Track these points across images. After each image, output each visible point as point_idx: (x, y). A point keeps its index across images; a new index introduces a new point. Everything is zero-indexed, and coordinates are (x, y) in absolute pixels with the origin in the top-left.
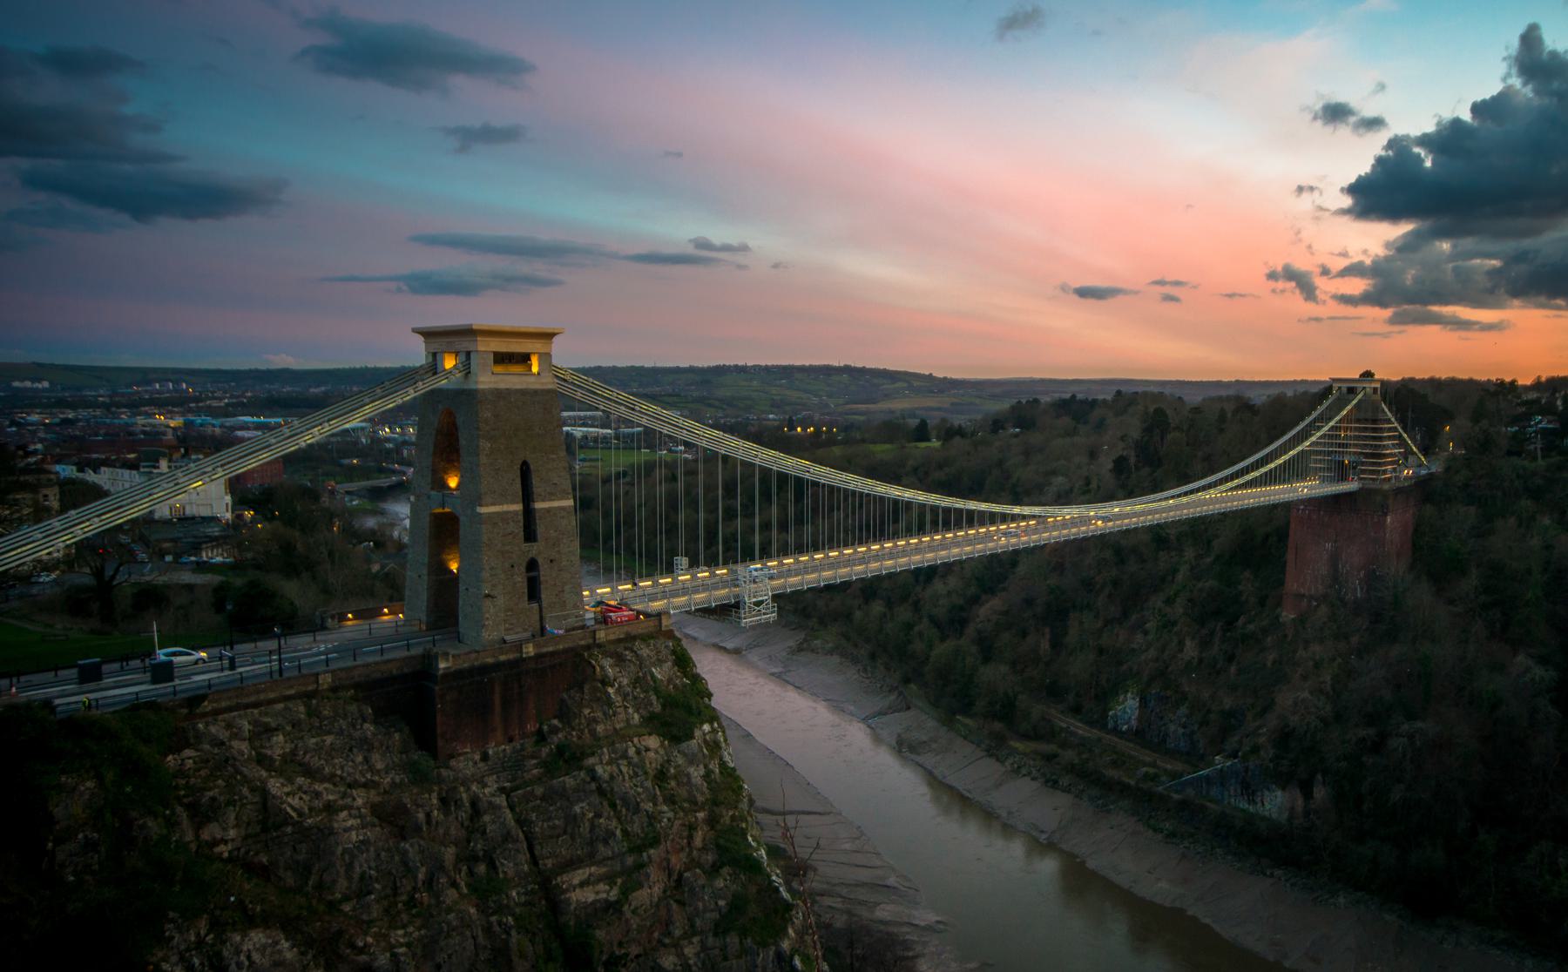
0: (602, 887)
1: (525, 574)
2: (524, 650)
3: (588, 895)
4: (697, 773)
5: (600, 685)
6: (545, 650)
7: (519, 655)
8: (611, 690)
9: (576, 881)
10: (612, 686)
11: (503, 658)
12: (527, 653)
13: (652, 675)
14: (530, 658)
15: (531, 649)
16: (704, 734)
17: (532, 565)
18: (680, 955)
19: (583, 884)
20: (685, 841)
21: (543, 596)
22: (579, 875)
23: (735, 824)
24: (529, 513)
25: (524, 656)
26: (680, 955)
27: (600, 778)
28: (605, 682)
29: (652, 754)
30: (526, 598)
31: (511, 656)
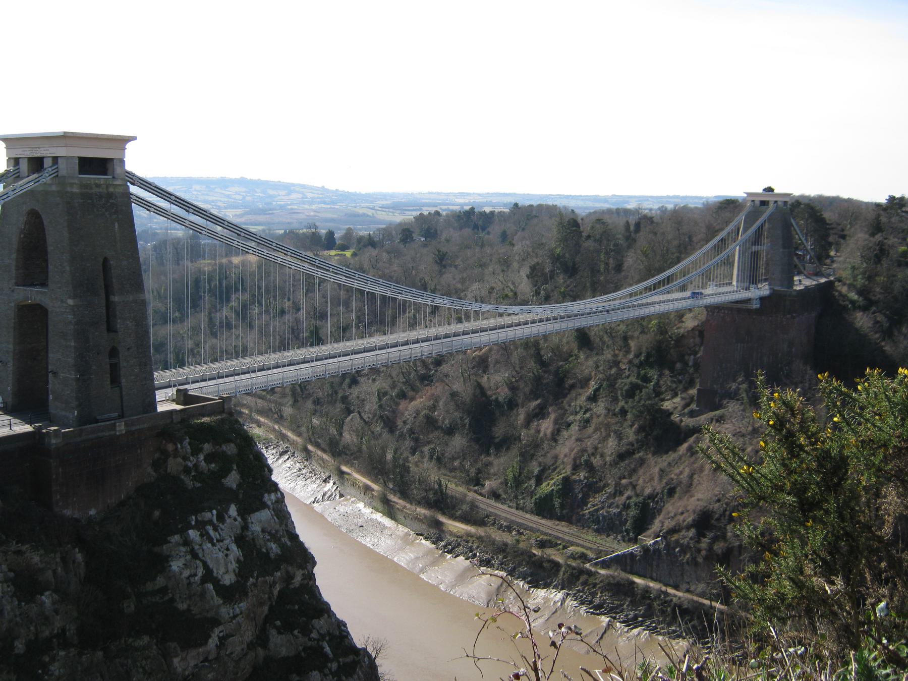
1: (108, 360)
2: (118, 429)
5: (181, 461)
6: (133, 428)
7: (113, 433)
12: (119, 431)
14: (122, 435)
15: (123, 428)
17: (114, 352)
20: (267, 596)
21: (123, 381)
23: (305, 582)
24: (109, 305)
25: (118, 433)
27: (192, 541)
30: (109, 382)
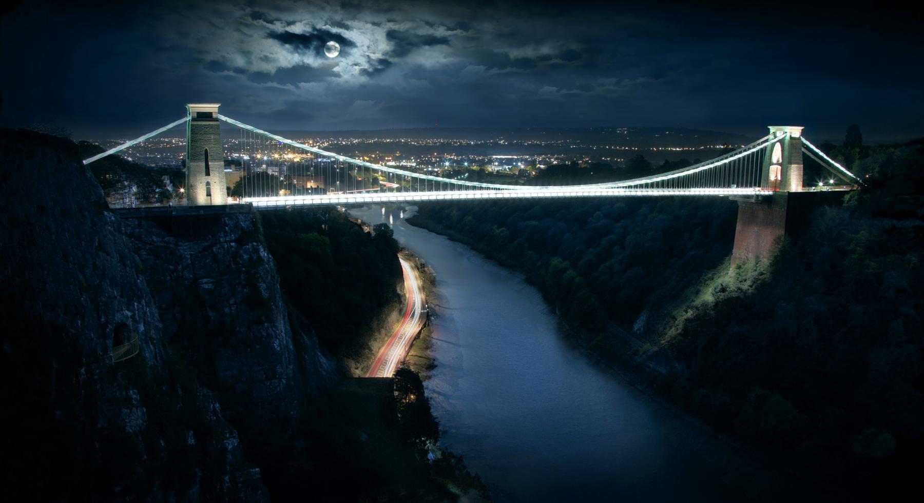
0: (210, 285)
3: (206, 286)
4: (246, 257)
8: (227, 228)
9: (204, 282)
10: (227, 227)
11: (193, 214)
13: (241, 224)
16: (253, 245)
18: (231, 309)
19: (205, 283)
22: (205, 280)
26: (231, 309)
28: (225, 225)
29: (233, 249)
31: (196, 214)
